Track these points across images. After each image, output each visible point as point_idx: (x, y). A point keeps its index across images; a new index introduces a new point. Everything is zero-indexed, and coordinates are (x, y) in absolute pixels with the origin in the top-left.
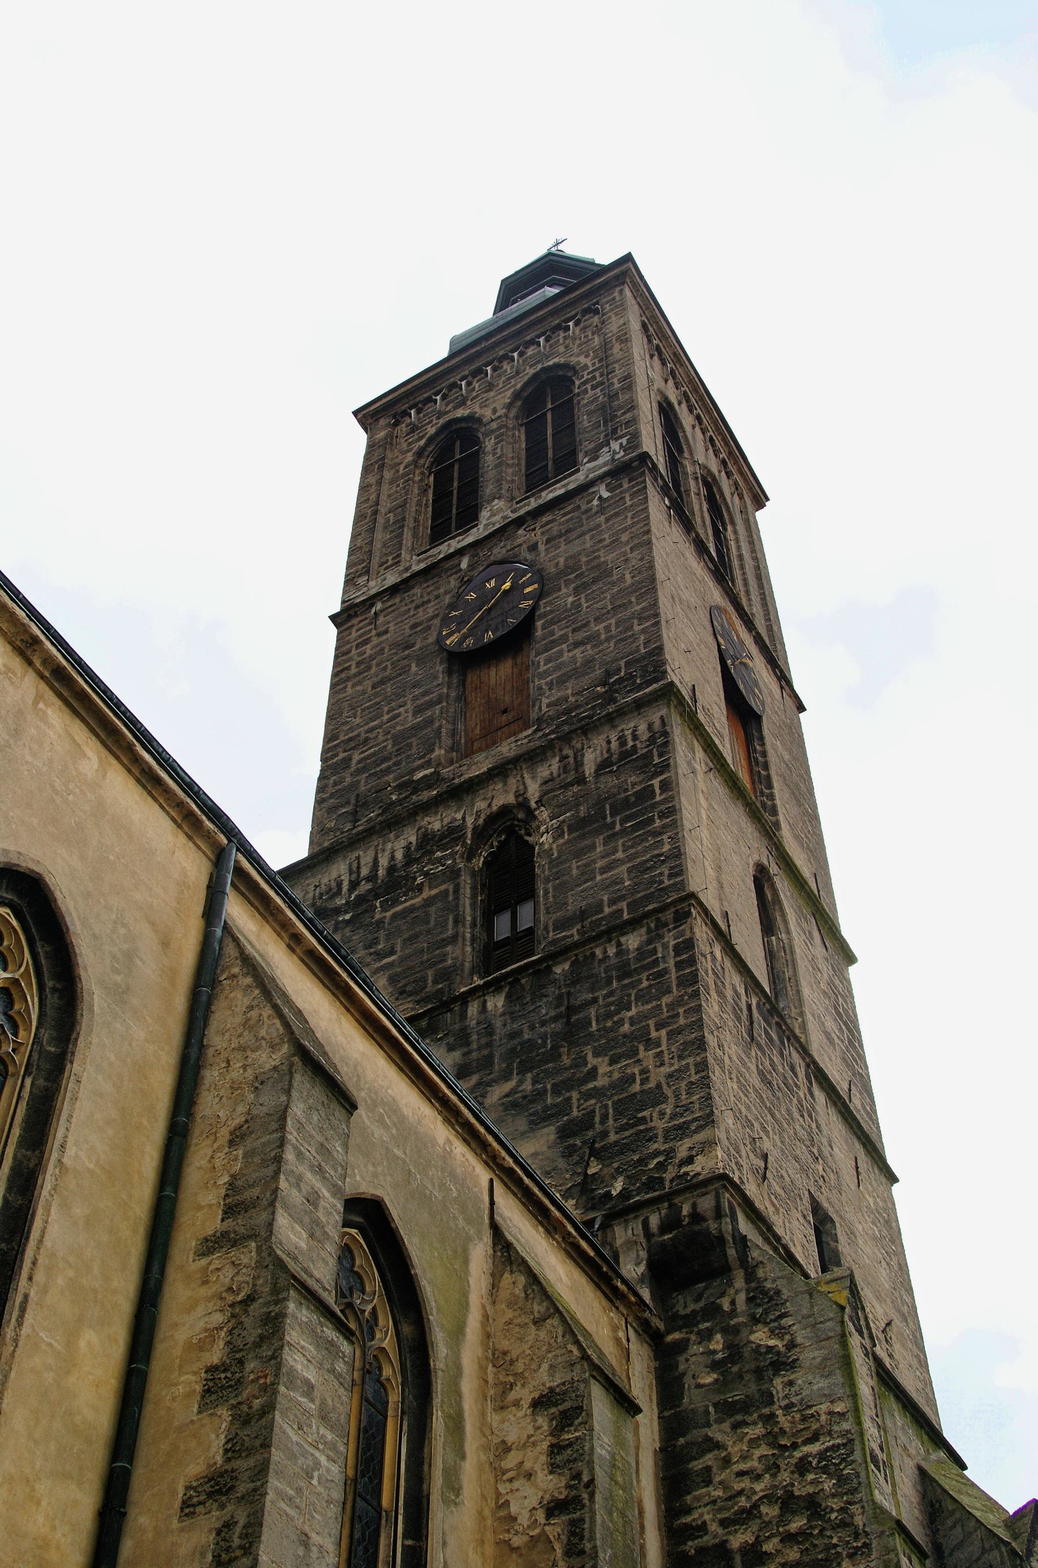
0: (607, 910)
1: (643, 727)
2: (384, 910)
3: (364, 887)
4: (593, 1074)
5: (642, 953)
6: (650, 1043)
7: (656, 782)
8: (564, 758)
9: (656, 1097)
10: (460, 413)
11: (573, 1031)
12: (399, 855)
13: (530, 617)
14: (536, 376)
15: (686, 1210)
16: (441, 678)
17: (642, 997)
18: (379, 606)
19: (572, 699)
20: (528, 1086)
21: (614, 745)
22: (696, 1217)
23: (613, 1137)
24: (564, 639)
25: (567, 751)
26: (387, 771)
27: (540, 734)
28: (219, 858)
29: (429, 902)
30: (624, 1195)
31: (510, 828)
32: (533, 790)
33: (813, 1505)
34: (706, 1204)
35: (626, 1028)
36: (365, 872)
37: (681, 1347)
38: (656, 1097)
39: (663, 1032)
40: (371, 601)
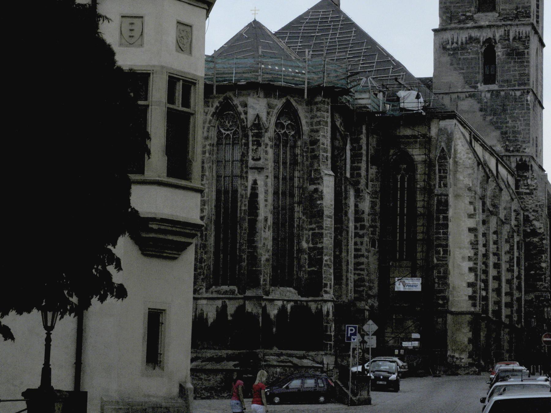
0: (513, 83)
1: (524, 31)
2: (461, 55)
3: (455, 45)
4: (507, 122)
6: (520, 120)
7: (526, 51)
8: (505, 30)
9: (519, 133)
11: (504, 110)
12: (464, 40)
15: (524, 159)
19: (508, 11)
20: (495, 120)
21: (517, 34)
22: (525, 161)
23: (511, 138)
25: (506, 29)
26: (459, 7)
27: (499, 18)
28: (497, 160)
29: (472, 59)
30: (513, 151)
31: (490, 44)
33: (537, 211)
34: (527, 159)
35: (515, 115)
36: (455, 40)
37: (520, 181)
38: (519, 133)
39: (522, 119)
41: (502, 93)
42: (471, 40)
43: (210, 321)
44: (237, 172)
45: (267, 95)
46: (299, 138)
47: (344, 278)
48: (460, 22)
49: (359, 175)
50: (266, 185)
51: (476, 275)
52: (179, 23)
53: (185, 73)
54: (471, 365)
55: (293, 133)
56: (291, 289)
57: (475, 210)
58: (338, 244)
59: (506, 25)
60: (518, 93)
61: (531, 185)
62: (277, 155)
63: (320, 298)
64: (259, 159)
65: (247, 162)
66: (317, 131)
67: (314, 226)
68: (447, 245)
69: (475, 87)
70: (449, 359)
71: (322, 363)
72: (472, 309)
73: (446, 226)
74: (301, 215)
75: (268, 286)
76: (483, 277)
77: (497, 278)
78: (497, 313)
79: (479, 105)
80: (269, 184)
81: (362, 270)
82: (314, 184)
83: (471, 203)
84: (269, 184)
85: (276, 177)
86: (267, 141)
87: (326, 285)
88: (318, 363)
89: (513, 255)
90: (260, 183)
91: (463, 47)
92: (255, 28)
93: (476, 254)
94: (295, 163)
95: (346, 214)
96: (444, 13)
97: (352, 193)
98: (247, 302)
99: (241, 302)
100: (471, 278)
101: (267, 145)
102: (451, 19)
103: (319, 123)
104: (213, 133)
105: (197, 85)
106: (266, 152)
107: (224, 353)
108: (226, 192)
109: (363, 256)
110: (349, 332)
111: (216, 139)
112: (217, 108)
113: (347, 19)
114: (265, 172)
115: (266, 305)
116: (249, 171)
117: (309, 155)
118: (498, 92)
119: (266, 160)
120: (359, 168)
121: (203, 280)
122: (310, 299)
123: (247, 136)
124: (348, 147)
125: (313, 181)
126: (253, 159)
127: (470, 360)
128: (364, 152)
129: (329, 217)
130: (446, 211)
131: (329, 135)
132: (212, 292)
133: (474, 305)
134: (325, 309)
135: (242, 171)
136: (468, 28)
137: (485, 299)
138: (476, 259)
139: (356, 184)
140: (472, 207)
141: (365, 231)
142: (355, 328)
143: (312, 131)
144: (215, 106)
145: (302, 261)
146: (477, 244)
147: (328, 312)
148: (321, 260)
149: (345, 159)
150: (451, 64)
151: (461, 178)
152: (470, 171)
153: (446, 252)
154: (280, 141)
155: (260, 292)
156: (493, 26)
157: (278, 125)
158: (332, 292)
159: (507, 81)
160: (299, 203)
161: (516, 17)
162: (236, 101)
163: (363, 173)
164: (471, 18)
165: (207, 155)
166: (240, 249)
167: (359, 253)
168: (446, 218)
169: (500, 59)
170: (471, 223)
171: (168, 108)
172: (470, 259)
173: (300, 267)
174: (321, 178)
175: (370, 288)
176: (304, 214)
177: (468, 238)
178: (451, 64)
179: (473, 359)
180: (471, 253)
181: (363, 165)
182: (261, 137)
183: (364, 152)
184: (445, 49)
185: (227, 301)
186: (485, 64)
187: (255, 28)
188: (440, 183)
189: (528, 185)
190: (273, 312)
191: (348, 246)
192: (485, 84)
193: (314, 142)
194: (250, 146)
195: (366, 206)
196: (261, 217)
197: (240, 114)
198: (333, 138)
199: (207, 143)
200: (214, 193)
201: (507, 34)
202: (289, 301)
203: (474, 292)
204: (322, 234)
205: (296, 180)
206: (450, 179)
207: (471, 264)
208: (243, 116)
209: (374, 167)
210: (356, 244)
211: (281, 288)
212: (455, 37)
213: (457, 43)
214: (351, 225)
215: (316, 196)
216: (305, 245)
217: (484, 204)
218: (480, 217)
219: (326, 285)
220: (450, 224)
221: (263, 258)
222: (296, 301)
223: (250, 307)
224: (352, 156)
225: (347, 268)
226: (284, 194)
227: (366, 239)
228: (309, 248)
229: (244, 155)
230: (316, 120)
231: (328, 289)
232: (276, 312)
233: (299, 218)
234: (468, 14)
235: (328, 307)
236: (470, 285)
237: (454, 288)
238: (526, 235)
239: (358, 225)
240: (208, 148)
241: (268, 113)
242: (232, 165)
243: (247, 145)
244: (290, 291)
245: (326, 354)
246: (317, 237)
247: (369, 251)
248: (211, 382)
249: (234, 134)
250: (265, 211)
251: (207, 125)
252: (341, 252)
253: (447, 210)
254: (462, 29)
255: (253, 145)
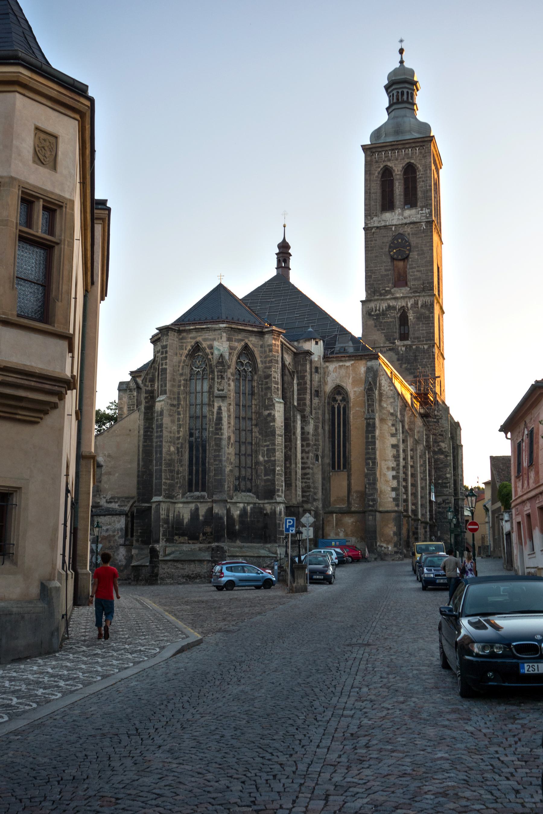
3: (378, 312)
5: (427, 350)
10: (389, 164)
11: (416, 360)
13: (409, 255)
14: (408, 163)
16: (390, 264)
17: (427, 358)
18: (373, 230)
24: (415, 268)
26: (380, 284)
29: (391, 322)
32: (409, 305)
33: (442, 435)
40: (372, 228)
41: (414, 347)
42: (389, 308)
43: (186, 521)
44: (206, 400)
45: (229, 339)
46: (256, 373)
47: (294, 484)
48: (381, 295)
49: (305, 404)
50: (229, 410)
51: (398, 482)
52: (37, 129)
53: (45, 190)
54: (396, 553)
55: (250, 370)
56: (251, 494)
57: (396, 430)
58: (288, 458)
59: (416, 297)
60: (426, 347)
61: (438, 416)
62: (238, 387)
63: (274, 501)
64: (223, 390)
65: (213, 392)
66: (270, 368)
67: (268, 443)
68: (375, 458)
69: (394, 343)
70: (379, 549)
71: (276, 553)
72: (396, 509)
73: (374, 443)
74: (257, 434)
75: (232, 492)
76: (404, 484)
77: (414, 485)
78: (415, 512)
79: (396, 357)
80: (232, 410)
81: (309, 479)
82: (268, 410)
83: (393, 425)
84: (232, 410)
85: (238, 405)
86: (229, 375)
87: (278, 490)
88: (273, 553)
89: (426, 467)
90: (224, 409)
91: (384, 314)
92: (220, 292)
93: (398, 465)
94: (252, 394)
95: (294, 434)
96: (369, 288)
97: (299, 417)
98: (214, 505)
99: (209, 505)
100: (394, 484)
101: (229, 379)
102: (374, 293)
103: (271, 361)
104: (187, 371)
105: (64, 209)
106: (229, 385)
107: (197, 546)
108: (197, 417)
109: (309, 468)
110: (288, 524)
111: (189, 375)
112: (190, 350)
113: (293, 286)
114: (228, 401)
115: (230, 508)
116: (215, 399)
117: (264, 386)
118: (411, 346)
119: (229, 391)
120: (305, 399)
121: (180, 487)
122: (266, 501)
123: (212, 372)
124: (295, 381)
125: (267, 408)
126: (219, 390)
127: (395, 549)
128: (308, 386)
129: (281, 436)
130: (374, 431)
131: (279, 371)
132: (187, 498)
133: (397, 505)
134: (278, 509)
135: (210, 400)
136: (387, 299)
137: (406, 501)
138: (399, 469)
139: (302, 411)
140: (394, 428)
141: (310, 448)
142: (293, 520)
143: (266, 368)
144: (188, 349)
145: (259, 471)
146: (399, 457)
147: (280, 512)
148: (274, 470)
149: (293, 391)
150: (376, 326)
151: (385, 405)
152: (392, 400)
153: (374, 463)
154: (240, 375)
155: (225, 496)
156: (406, 297)
157: (239, 363)
158: (283, 496)
159: (418, 338)
160: (256, 425)
161: (424, 290)
162: (205, 345)
163: (308, 402)
164: (389, 292)
165: (182, 388)
166: (209, 462)
167: (306, 466)
168: (374, 437)
169: (411, 321)
170: (394, 441)
171: (20, 231)
172: (393, 469)
173: (258, 476)
174: (273, 405)
175: (315, 494)
176: (260, 434)
177: (390, 453)
178: (376, 326)
179: (398, 548)
180: (392, 464)
181: (308, 397)
182: (224, 372)
183: (308, 386)
184: (370, 315)
185: (199, 504)
186: (400, 326)
187: (220, 292)
188: (368, 410)
189: (435, 416)
190: (236, 513)
191: (296, 459)
192: (401, 340)
193: (268, 376)
194: (216, 379)
195: (310, 428)
196: (225, 436)
197: (207, 355)
198: (283, 375)
199: (182, 379)
200: (188, 418)
201: (416, 303)
202: (248, 503)
203: (397, 495)
204: (275, 449)
205: (254, 406)
206: (377, 406)
207: (394, 473)
208: (210, 357)
209: (316, 398)
210: (302, 458)
211: (243, 493)
212: (378, 306)
213: (379, 310)
214: (299, 442)
215: (269, 419)
216: (261, 458)
217: (403, 427)
218: (401, 436)
219: (278, 490)
220: (377, 442)
221: (228, 469)
222: (255, 503)
223: (218, 509)
224: (298, 390)
225: (296, 477)
226: (244, 418)
227: (311, 455)
228: (265, 461)
229: (211, 387)
230: (268, 359)
231: (280, 494)
232: (238, 512)
233: (257, 437)
234: (387, 289)
235: (281, 508)
236: (393, 489)
237: (381, 492)
238: (435, 453)
239: (305, 443)
240: (183, 382)
241: (230, 354)
242: (202, 395)
243: (213, 379)
244: (250, 496)
245: (279, 546)
246: (272, 451)
247: (314, 464)
248: (186, 570)
249: (203, 371)
250: (227, 431)
251: (182, 364)
252: (291, 464)
253: (375, 430)
254: (382, 300)
255: (218, 379)
